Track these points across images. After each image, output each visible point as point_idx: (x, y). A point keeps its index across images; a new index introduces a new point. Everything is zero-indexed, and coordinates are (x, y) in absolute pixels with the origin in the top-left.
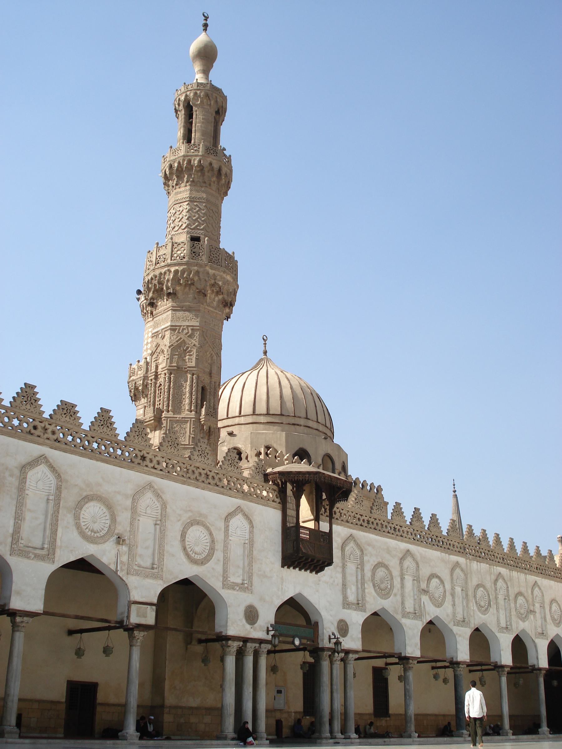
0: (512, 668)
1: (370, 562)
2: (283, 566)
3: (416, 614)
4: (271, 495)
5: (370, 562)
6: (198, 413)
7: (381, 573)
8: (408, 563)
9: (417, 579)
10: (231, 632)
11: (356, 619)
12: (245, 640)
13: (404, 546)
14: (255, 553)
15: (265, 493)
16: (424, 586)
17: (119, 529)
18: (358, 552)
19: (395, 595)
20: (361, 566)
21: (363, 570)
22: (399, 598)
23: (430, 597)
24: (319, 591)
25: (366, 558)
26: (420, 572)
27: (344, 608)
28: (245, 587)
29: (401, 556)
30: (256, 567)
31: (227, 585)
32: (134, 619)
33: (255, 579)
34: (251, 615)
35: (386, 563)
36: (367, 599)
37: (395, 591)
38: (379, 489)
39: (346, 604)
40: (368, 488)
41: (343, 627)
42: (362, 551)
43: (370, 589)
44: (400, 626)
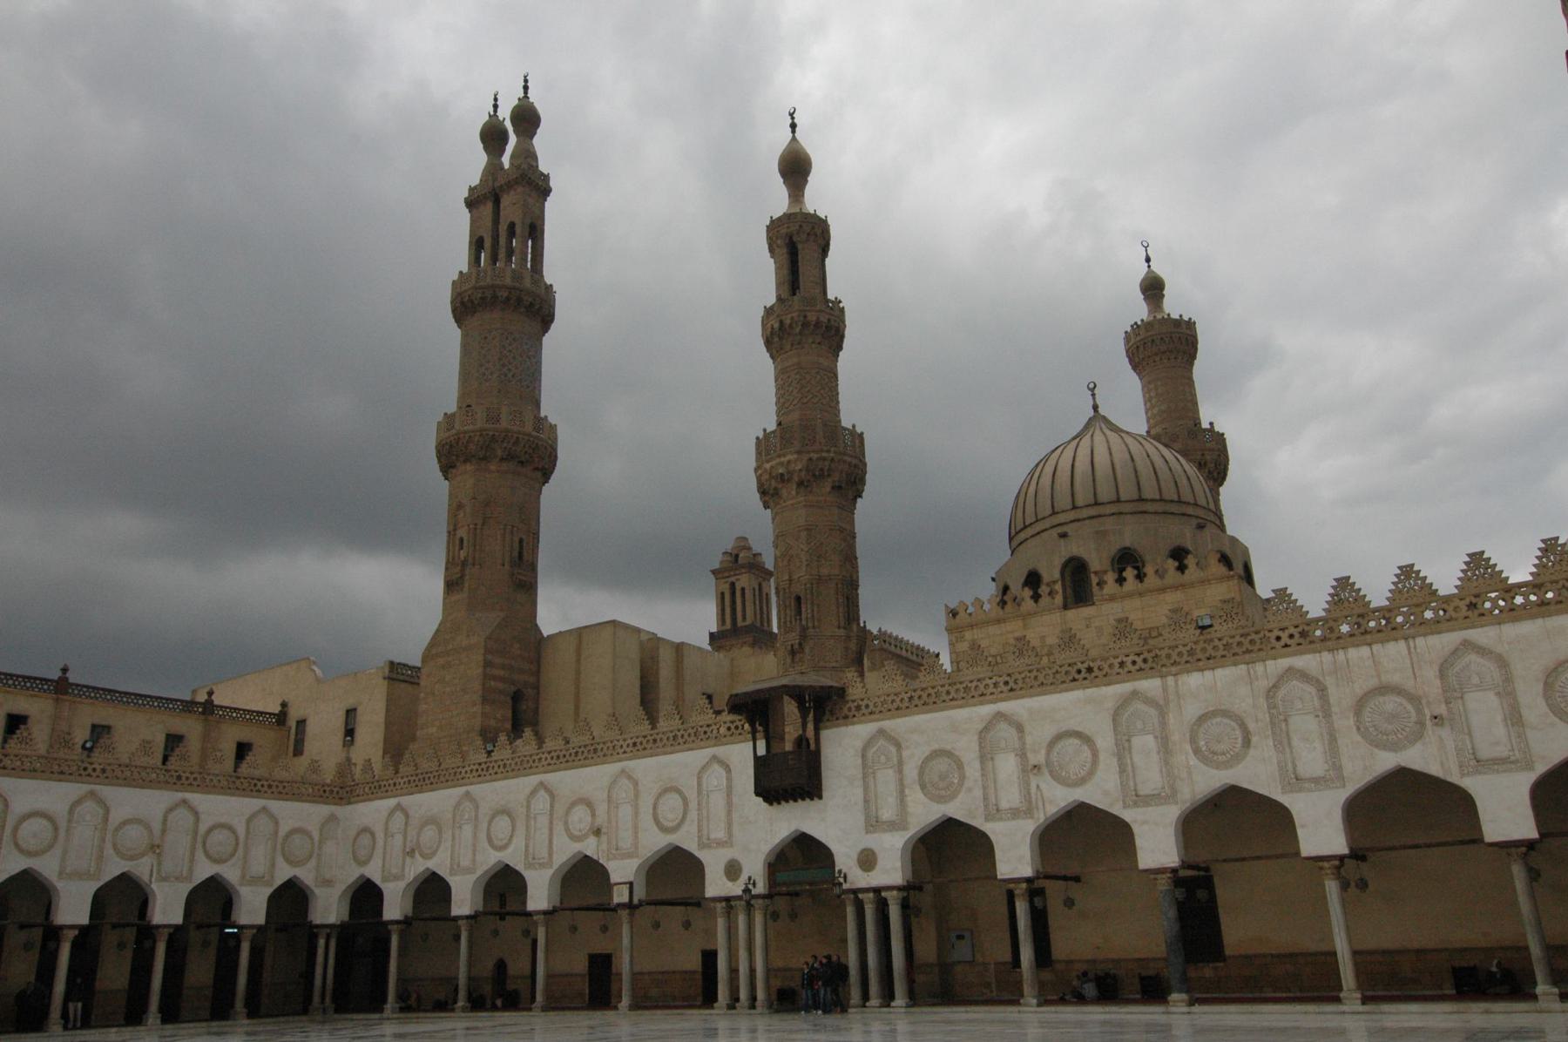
1: (914, 758)
5: (914, 758)
7: (942, 765)
8: (1005, 732)
9: (1022, 755)
10: (710, 892)
13: (987, 710)
14: (735, 800)
16: (1040, 758)
17: (599, 821)
18: (893, 749)
19: (970, 790)
21: (900, 771)
22: (978, 793)
25: (905, 754)
26: (1029, 739)
29: (980, 727)
30: (735, 816)
32: (616, 900)
33: (736, 829)
34: (733, 870)
35: (948, 747)
36: (910, 810)
37: (968, 783)
39: (873, 824)
42: (898, 746)
43: (915, 797)
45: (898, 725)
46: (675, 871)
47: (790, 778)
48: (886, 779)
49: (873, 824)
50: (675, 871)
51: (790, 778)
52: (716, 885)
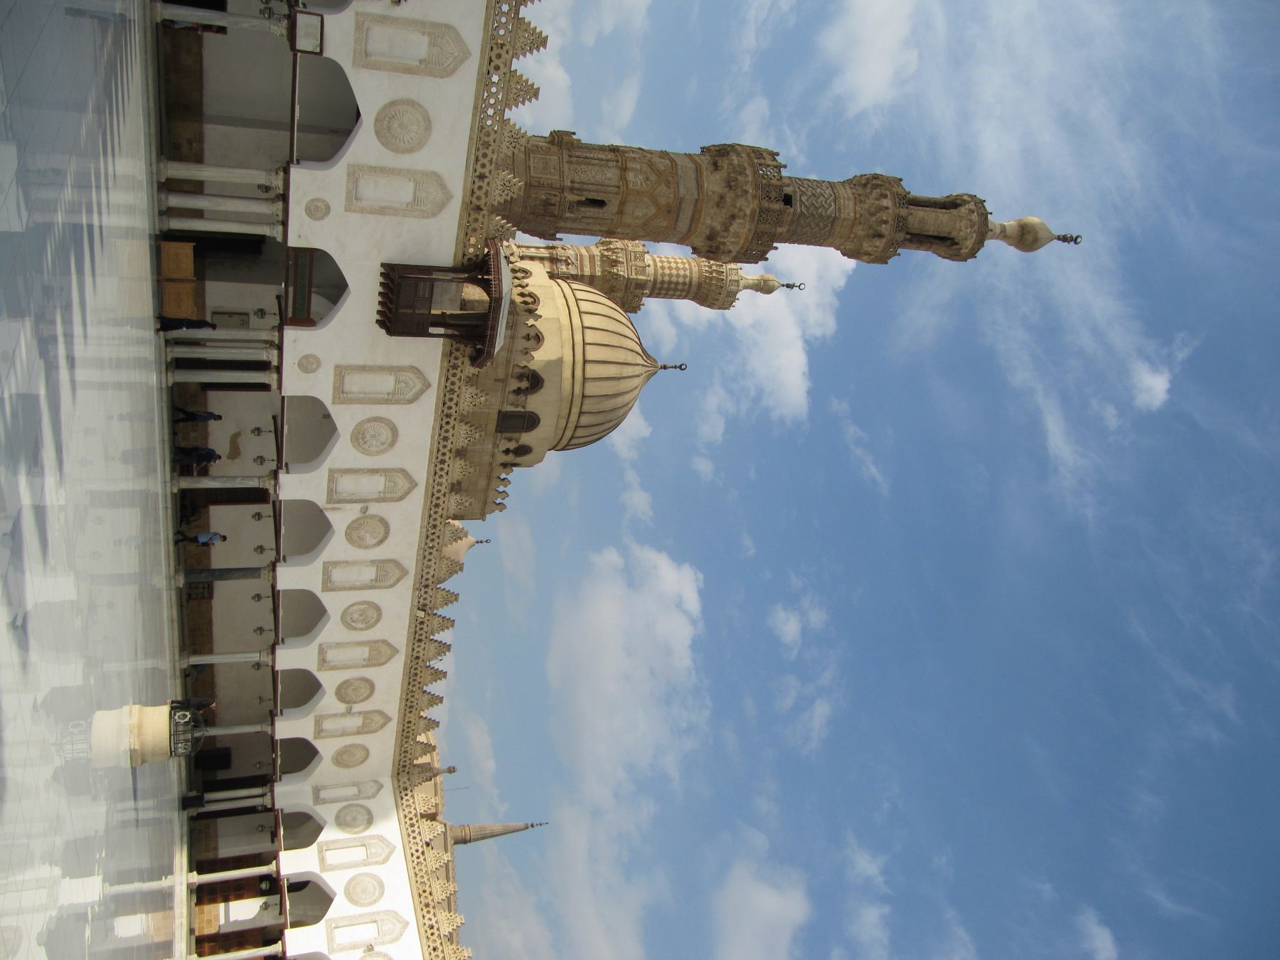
0: (272, 737)
2: (383, 265)
3: (334, 496)
4: (471, 250)
6: (572, 189)
7: (386, 434)
8: (402, 484)
11: (320, 387)
12: (284, 198)
15: (473, 240)
18: (410, 395)
20: (390, 400)
23: (358, 519)
24: (353, 324)
27: (337, 367)
28: (353, 199)
31: (354, 174)
38: (501, 507)
40: (501, 489)
41: (308, 364)
44: (318, 467)
45: (430, 401)
46: (329, 123)
47: (405, 300)
48: (386, 383)
49: (341, 372)
50: (329, 123)
51: (405, 300)
52: (304, 181)
